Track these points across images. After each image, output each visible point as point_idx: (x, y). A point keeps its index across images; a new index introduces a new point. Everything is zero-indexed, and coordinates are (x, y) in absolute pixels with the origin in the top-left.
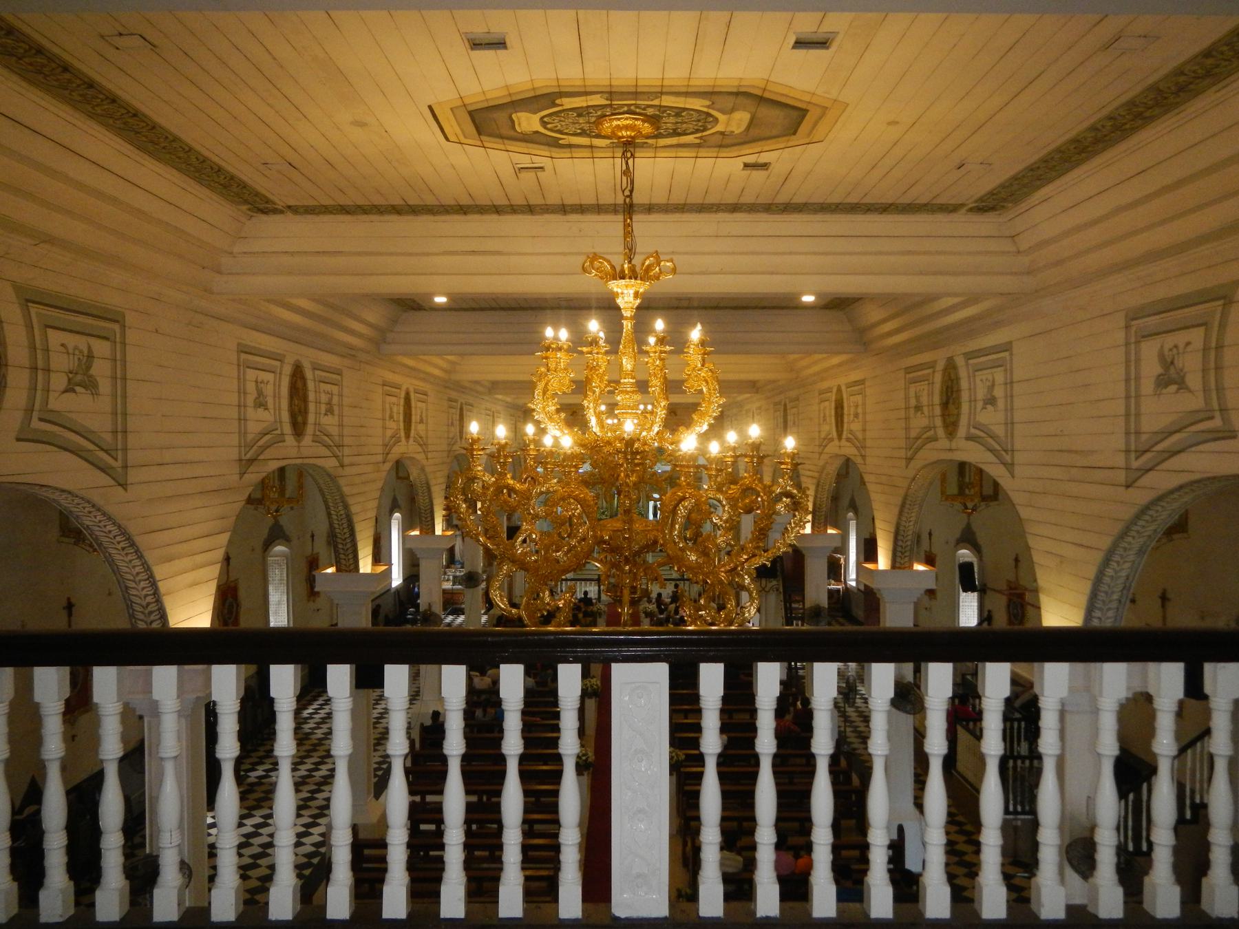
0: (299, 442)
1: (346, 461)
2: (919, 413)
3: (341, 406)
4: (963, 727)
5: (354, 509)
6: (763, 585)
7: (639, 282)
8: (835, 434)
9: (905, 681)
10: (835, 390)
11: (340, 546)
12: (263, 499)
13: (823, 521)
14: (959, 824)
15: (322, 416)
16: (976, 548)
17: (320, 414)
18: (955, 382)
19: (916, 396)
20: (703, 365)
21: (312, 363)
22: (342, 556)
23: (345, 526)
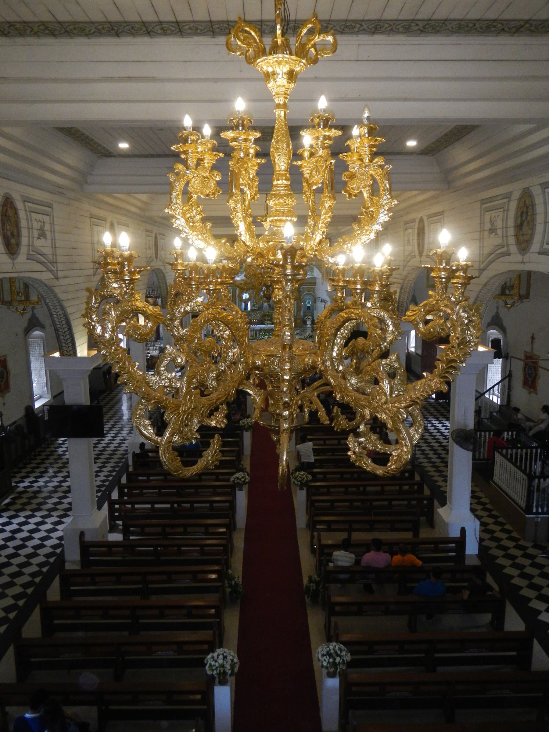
0: (13, 259)
1: (60, 274)
2: (494, 234)
3: (53, 231)
4: (501, 454)
5: (69, 310)
7: (294, 57)
8: (417, 253)
9: (468, 429)
10: (417, 221)
11: (62, 337)
12: (12, 301)
14: (478, 498)
15: (35, 239)
16: (502, 329)
17: (33, 237)
18: (530, 207)
19: (491, 221)
20: (371, 161)
21: (22, 196)
23: (64, 322)
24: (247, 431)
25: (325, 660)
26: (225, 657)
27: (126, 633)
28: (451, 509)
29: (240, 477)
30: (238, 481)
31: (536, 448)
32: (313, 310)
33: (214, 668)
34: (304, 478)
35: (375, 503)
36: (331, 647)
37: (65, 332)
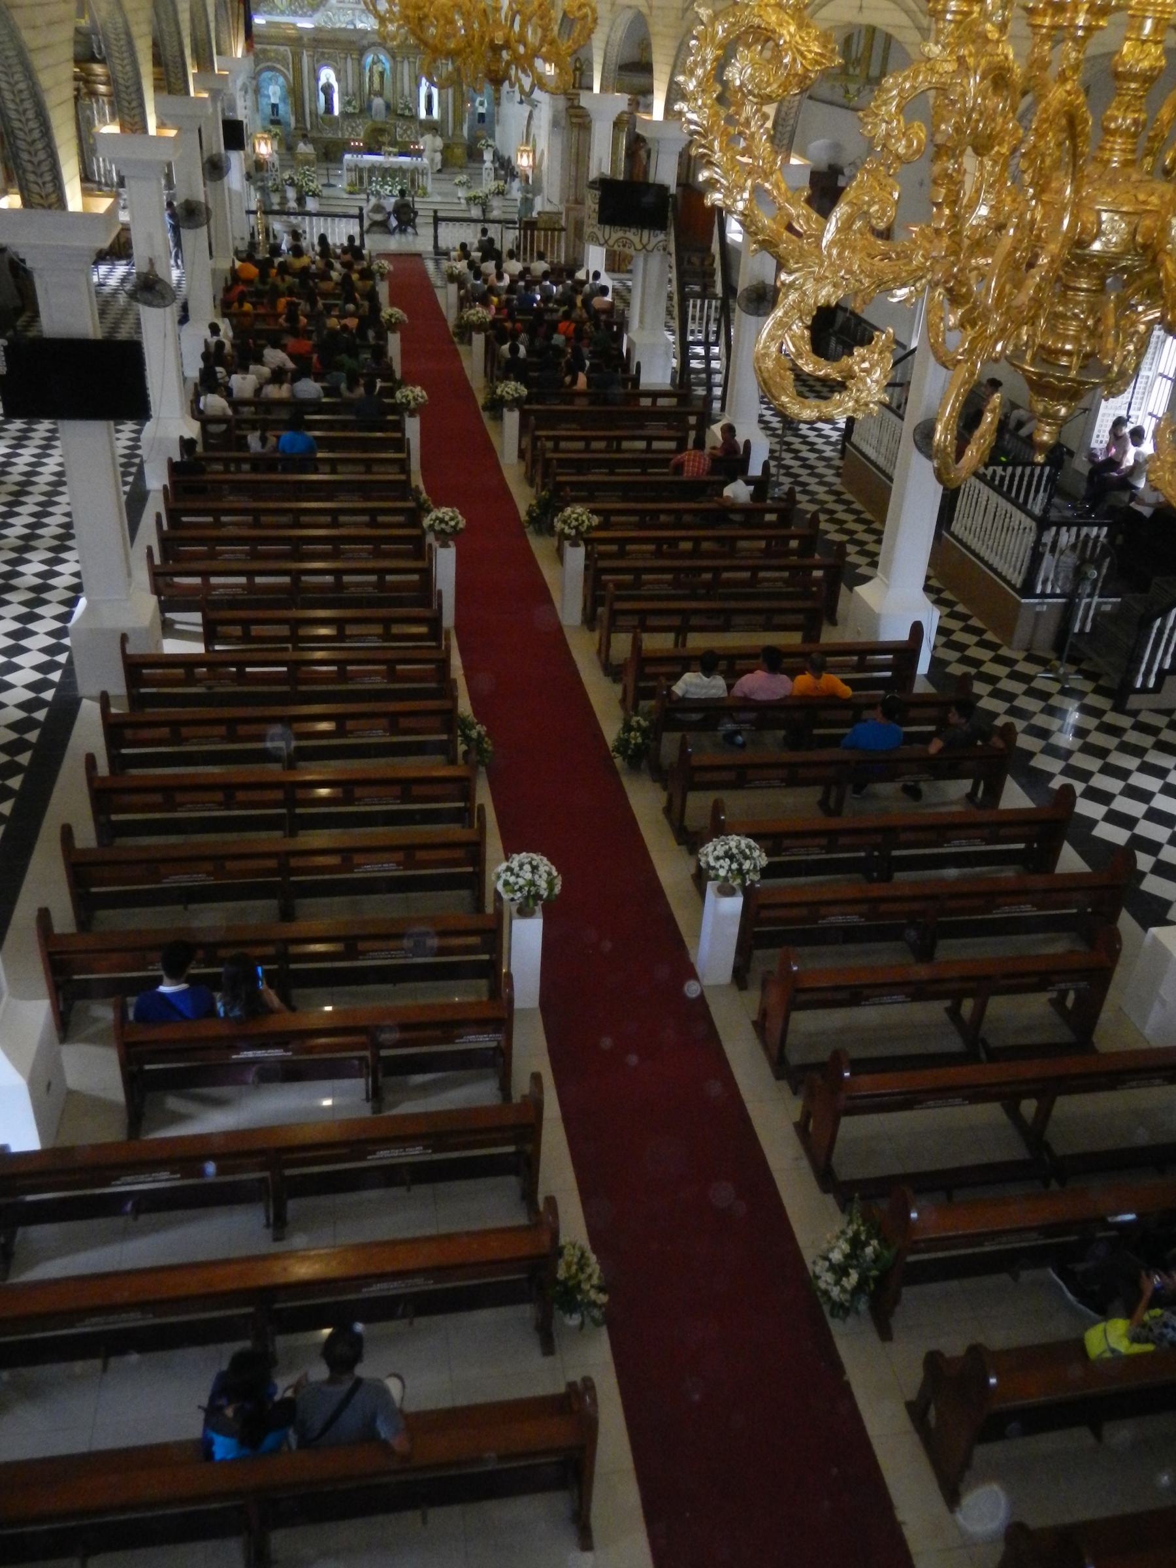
6: (645, 240)
11: (25, 156)
13: (785, 142)
22: (31, 177)
23: (31, 114)
24: (412, 415)
25: (721, 867)
26: (534, 869)
27: (278, 834)
28: (887, 586)
29: (447, 518)
30: (443, 526)
31: (1043, 466)
32: (492, 124)
33: (516, 887)
34: (583, 522)
35: (726, 575)
36: (733, 844)
37: (34, 141)
